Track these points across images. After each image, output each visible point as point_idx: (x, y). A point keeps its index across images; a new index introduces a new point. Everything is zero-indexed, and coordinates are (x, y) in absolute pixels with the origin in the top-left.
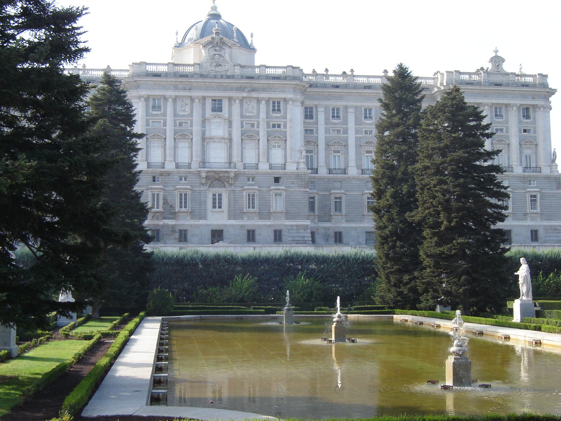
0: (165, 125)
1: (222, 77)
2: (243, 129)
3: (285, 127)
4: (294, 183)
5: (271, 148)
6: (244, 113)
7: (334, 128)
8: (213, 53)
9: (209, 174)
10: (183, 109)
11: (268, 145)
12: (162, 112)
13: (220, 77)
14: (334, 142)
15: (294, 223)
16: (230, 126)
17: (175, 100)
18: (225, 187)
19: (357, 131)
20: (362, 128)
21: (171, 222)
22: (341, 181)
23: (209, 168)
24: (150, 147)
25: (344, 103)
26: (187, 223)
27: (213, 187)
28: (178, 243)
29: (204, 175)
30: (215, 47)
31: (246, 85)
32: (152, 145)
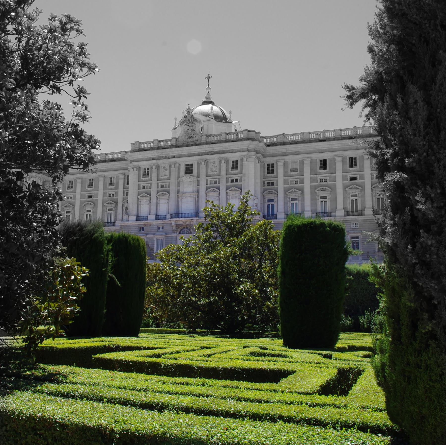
0: (150, 188)
1: (192, 145)
2: (207, 185)
5: (229, 199)
6: (209, 173)
8: (186, 128)
9: (179, 223)
11: (227, 198)
12: (149, 178)
16: (198, 185)
17: (158, 168)
18: (191, 233)
20: (317, 178)
24: (140, 205)
27: (183, 233)
29: (173, 224)
30: (188, 123)
31: (208, 149)
32: (142, 203)
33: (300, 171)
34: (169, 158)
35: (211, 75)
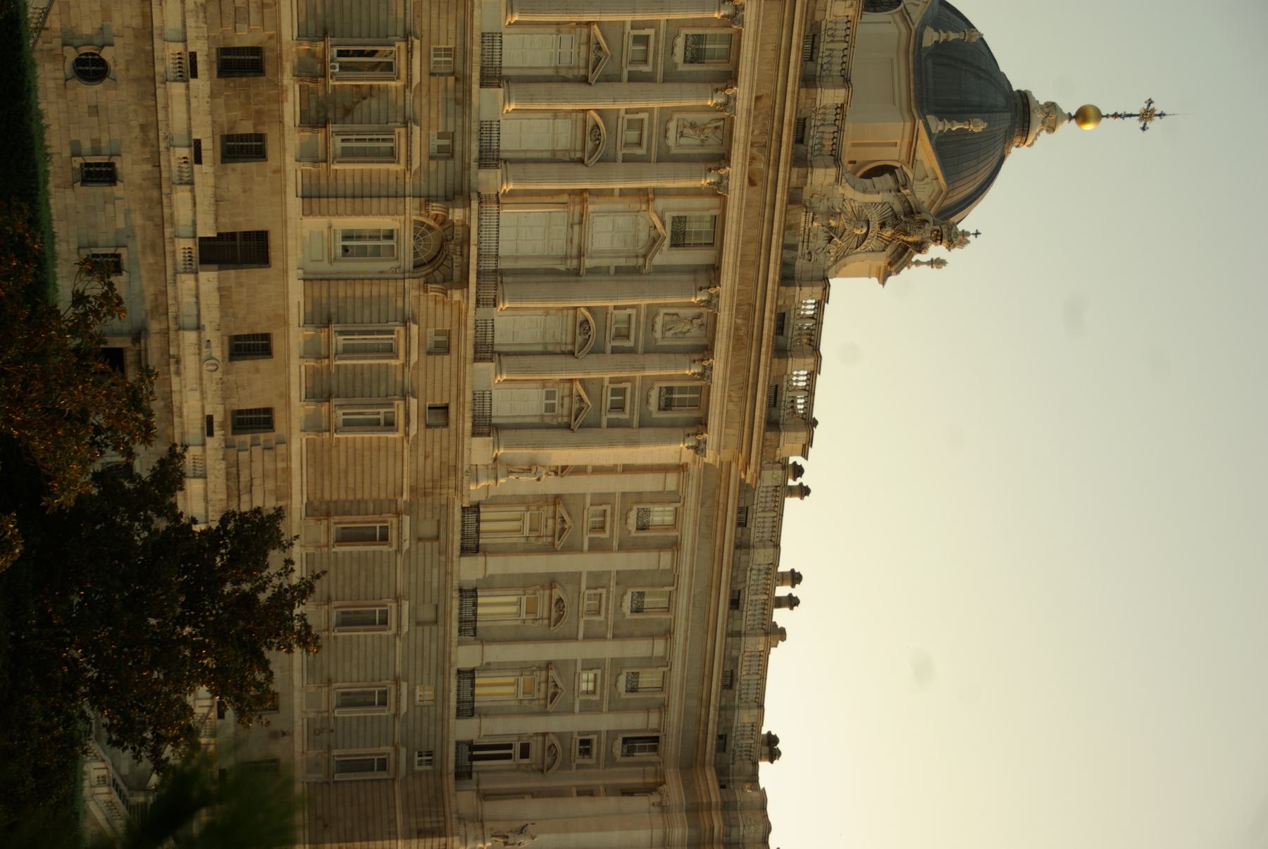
0: (634, 78)
3: (612, 425)
4: (429, 460)
6: (663, 311)
7: (612, 514)
10: (687, 131)
13: (789, 241)
14: (566, 517)
15: (295, 465)
19: (597, 579)
21: (291, 109)
22: (437, 538)
23: (480, 226)
24: (559, 32)
25: (687, 543)
26: (290, 160)
28: (218, 137)
32: (566, 37)
33: (637, 537)
34: (753, 159)
35: (1155, 124)
